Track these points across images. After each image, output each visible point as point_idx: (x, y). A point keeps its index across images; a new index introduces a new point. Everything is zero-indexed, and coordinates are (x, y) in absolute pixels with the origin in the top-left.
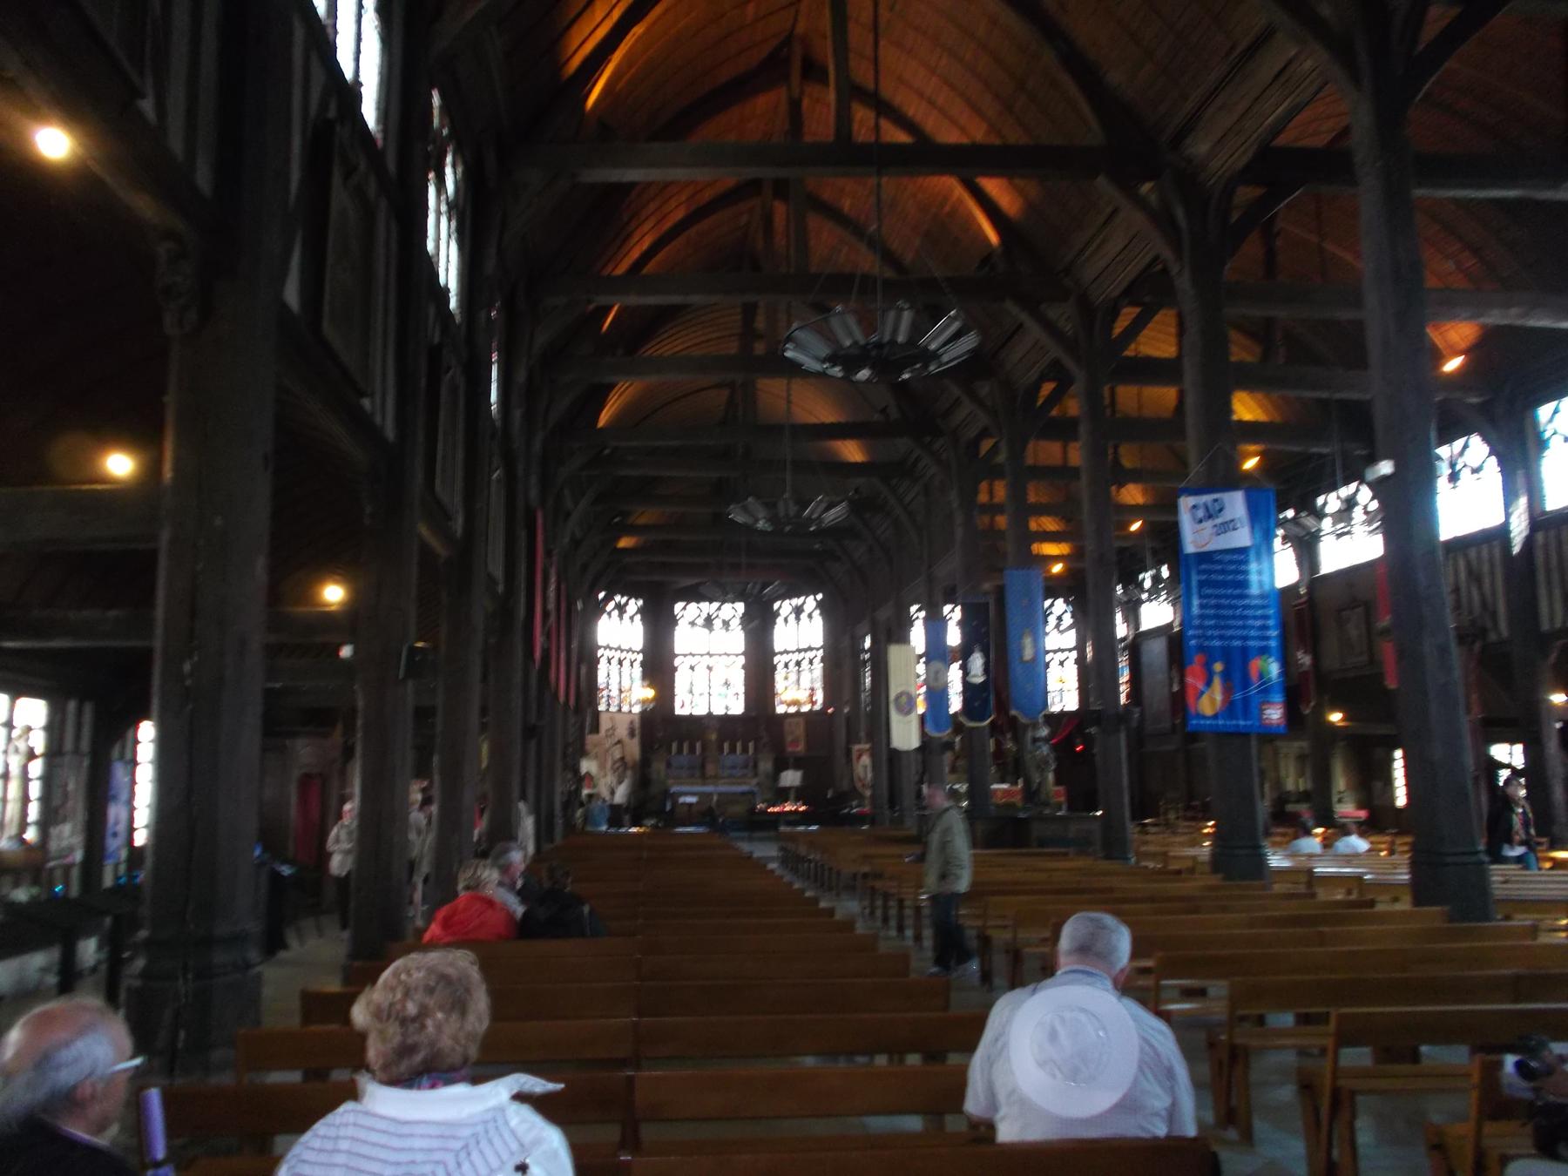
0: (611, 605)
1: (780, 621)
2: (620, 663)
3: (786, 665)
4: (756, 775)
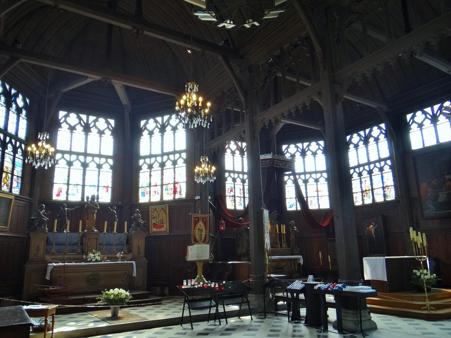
1: (145, 133)
3: (150, 167)
4: (130, 251)
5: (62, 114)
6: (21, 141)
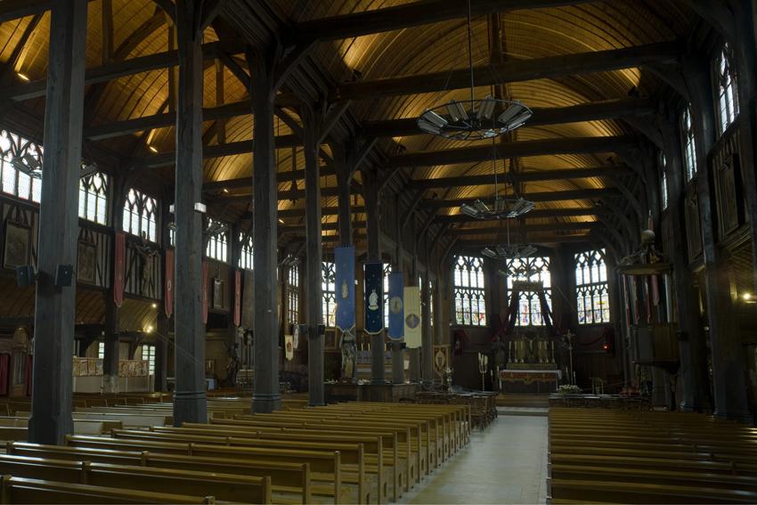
0: (461, 261)
2: (470, 297)
5: (508, 261)
6: (481, 289)
